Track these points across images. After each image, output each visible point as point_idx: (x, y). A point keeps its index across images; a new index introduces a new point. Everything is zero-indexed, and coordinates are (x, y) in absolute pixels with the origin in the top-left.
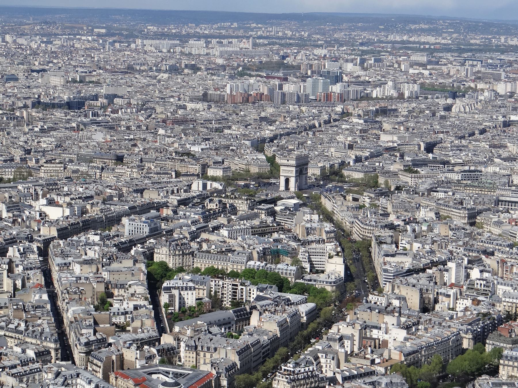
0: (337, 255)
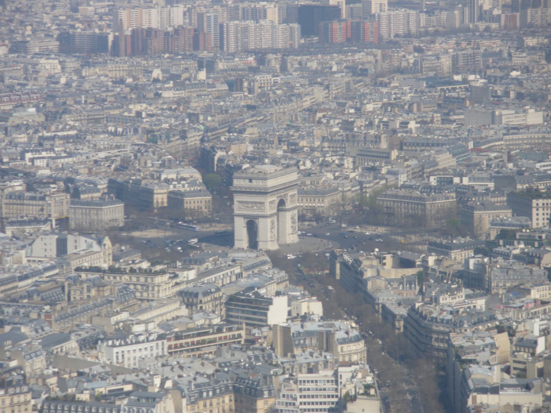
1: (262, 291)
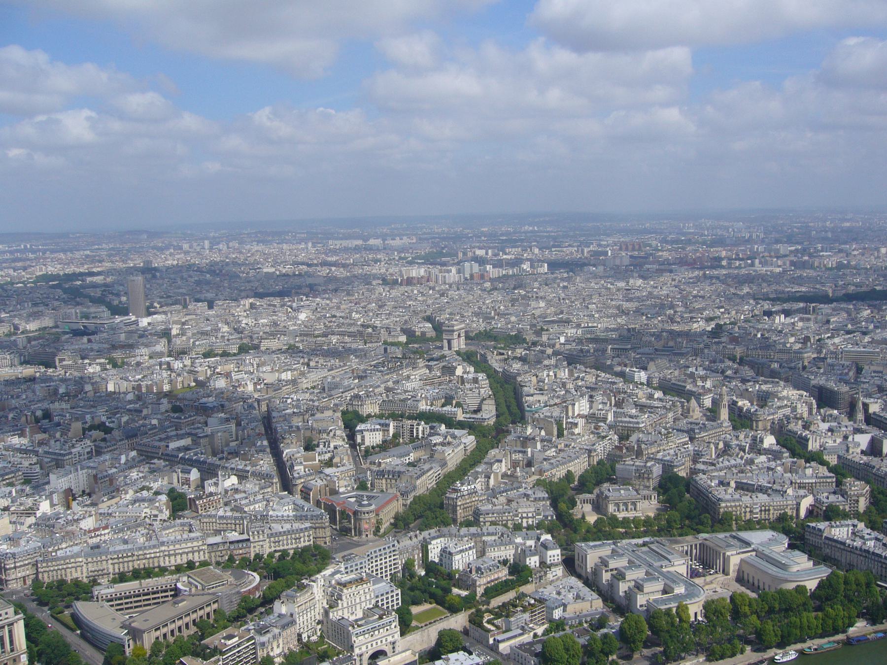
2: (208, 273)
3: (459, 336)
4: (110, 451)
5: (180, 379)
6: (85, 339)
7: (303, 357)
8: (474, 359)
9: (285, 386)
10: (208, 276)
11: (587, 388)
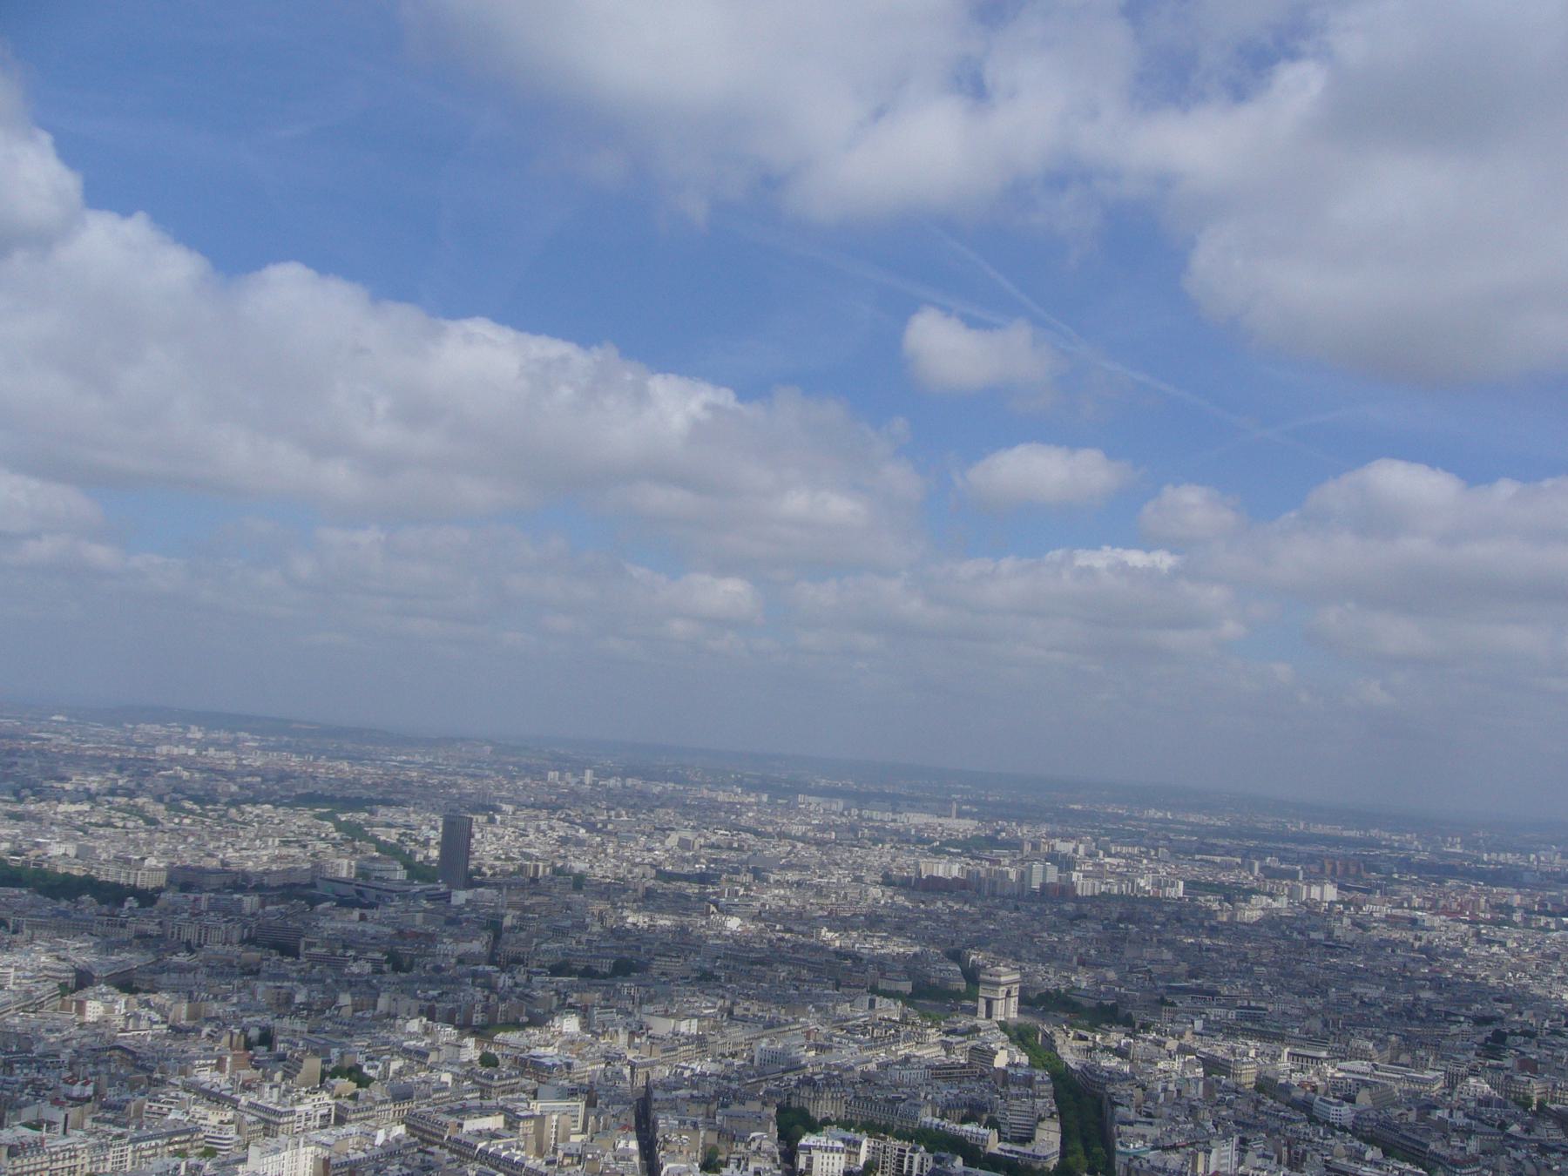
0: (1051, 1116)
1: (992, 1046)
2: (583, 826)
3: (1008, 994)
4: (362, 1119)
5: (502, 1007)
6: (356, 914)
7: (723, 997)
8: (1031, 1040)
9: (684, 1044)
10: (582, 831)
11: (1236, 1123)
